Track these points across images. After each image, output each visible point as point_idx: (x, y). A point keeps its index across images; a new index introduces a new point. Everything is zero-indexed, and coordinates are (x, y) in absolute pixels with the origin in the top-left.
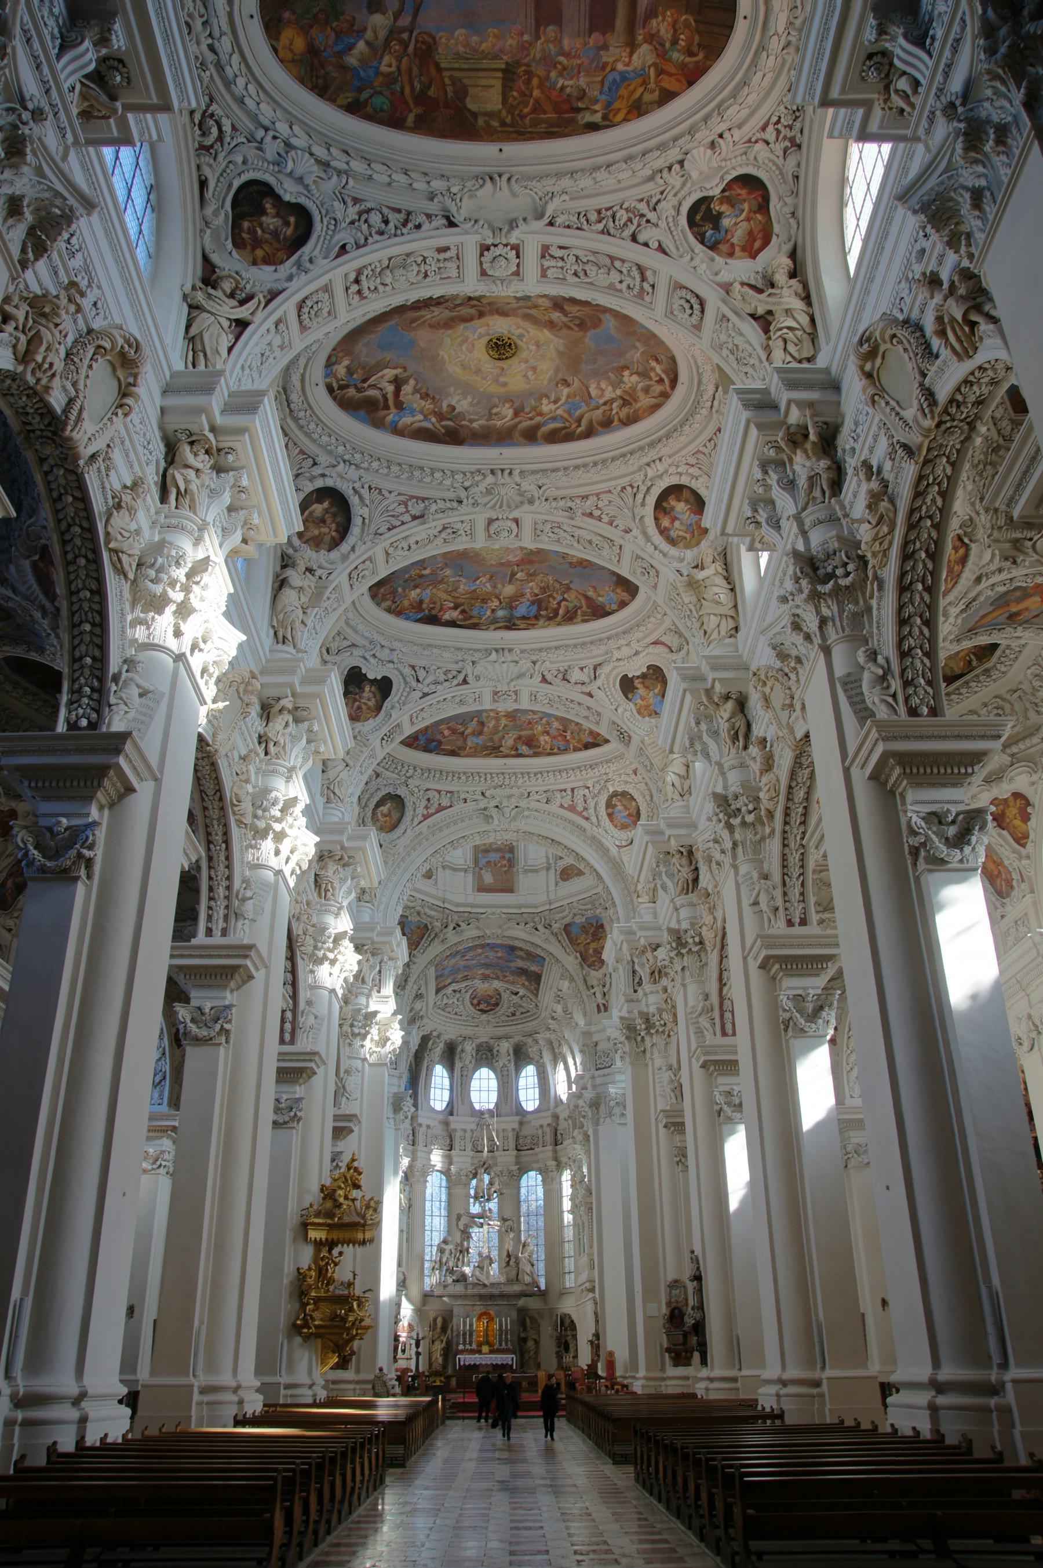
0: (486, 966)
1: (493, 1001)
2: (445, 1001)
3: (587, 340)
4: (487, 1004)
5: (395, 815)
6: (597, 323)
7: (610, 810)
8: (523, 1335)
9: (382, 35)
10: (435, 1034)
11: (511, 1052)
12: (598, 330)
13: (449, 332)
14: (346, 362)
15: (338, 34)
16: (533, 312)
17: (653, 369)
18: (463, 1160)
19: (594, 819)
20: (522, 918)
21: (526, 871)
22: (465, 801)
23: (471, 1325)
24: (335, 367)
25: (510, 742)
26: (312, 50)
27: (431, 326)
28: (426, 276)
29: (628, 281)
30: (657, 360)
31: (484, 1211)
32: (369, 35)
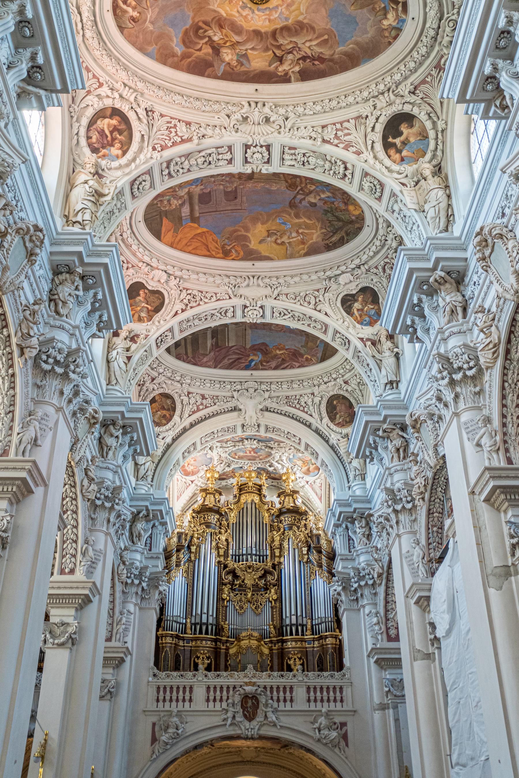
3: (191, 14)
6: (186, 41)
9: (312, 195)
12: (184, 28)
13: (301, 18)
14: (385, 23)
15: (333, 203)
16: (236, 38)
17: (134, 8)
24: (394, 24)
26: (346, 204)
27: (313, 29)
28: (304, 155)
29: (177, 168)
30: (133, 19)
32: (318, 198)
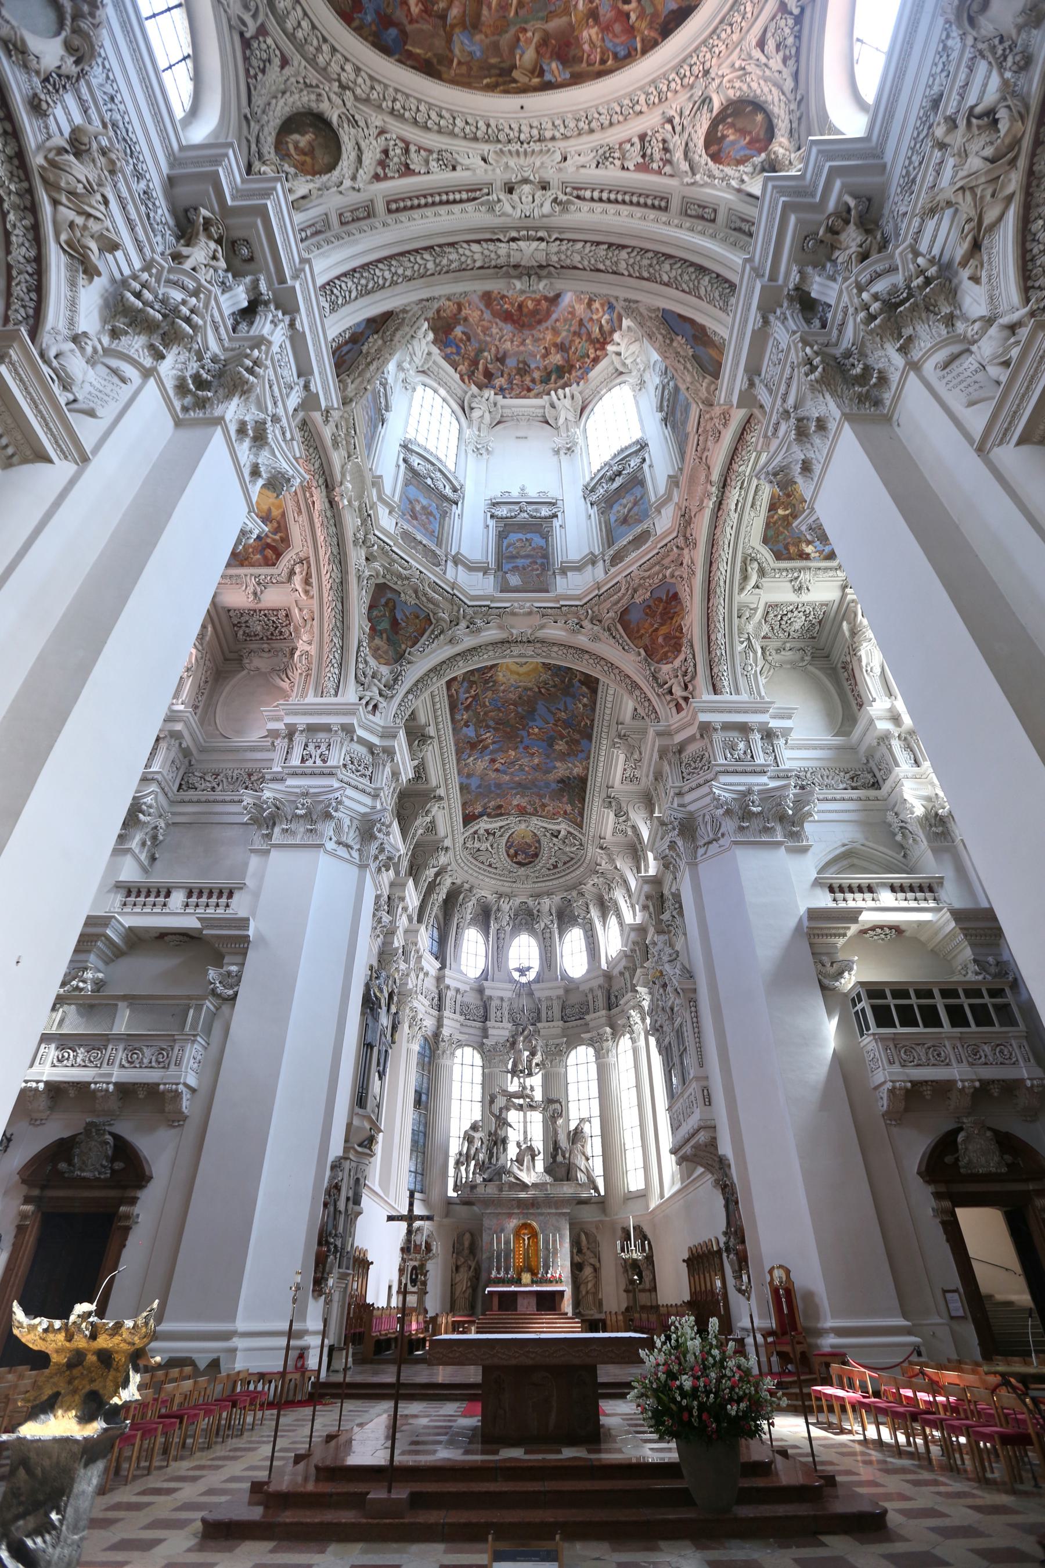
0: (522, 787)
1: (532, 851)
2: (477, 845)
4: (524, 854)
5: (322, 159)
7: (714, 149)
8: (577, 1259)
10: (466, 886)
11: (554, 911)
18: (500, 1031)
19: (684, 166)
20: (559, 612)
21: (564, 571)
22: (454, 168)
23: (507, 1243)
25: (528, 56)
31: (524, 1088)
